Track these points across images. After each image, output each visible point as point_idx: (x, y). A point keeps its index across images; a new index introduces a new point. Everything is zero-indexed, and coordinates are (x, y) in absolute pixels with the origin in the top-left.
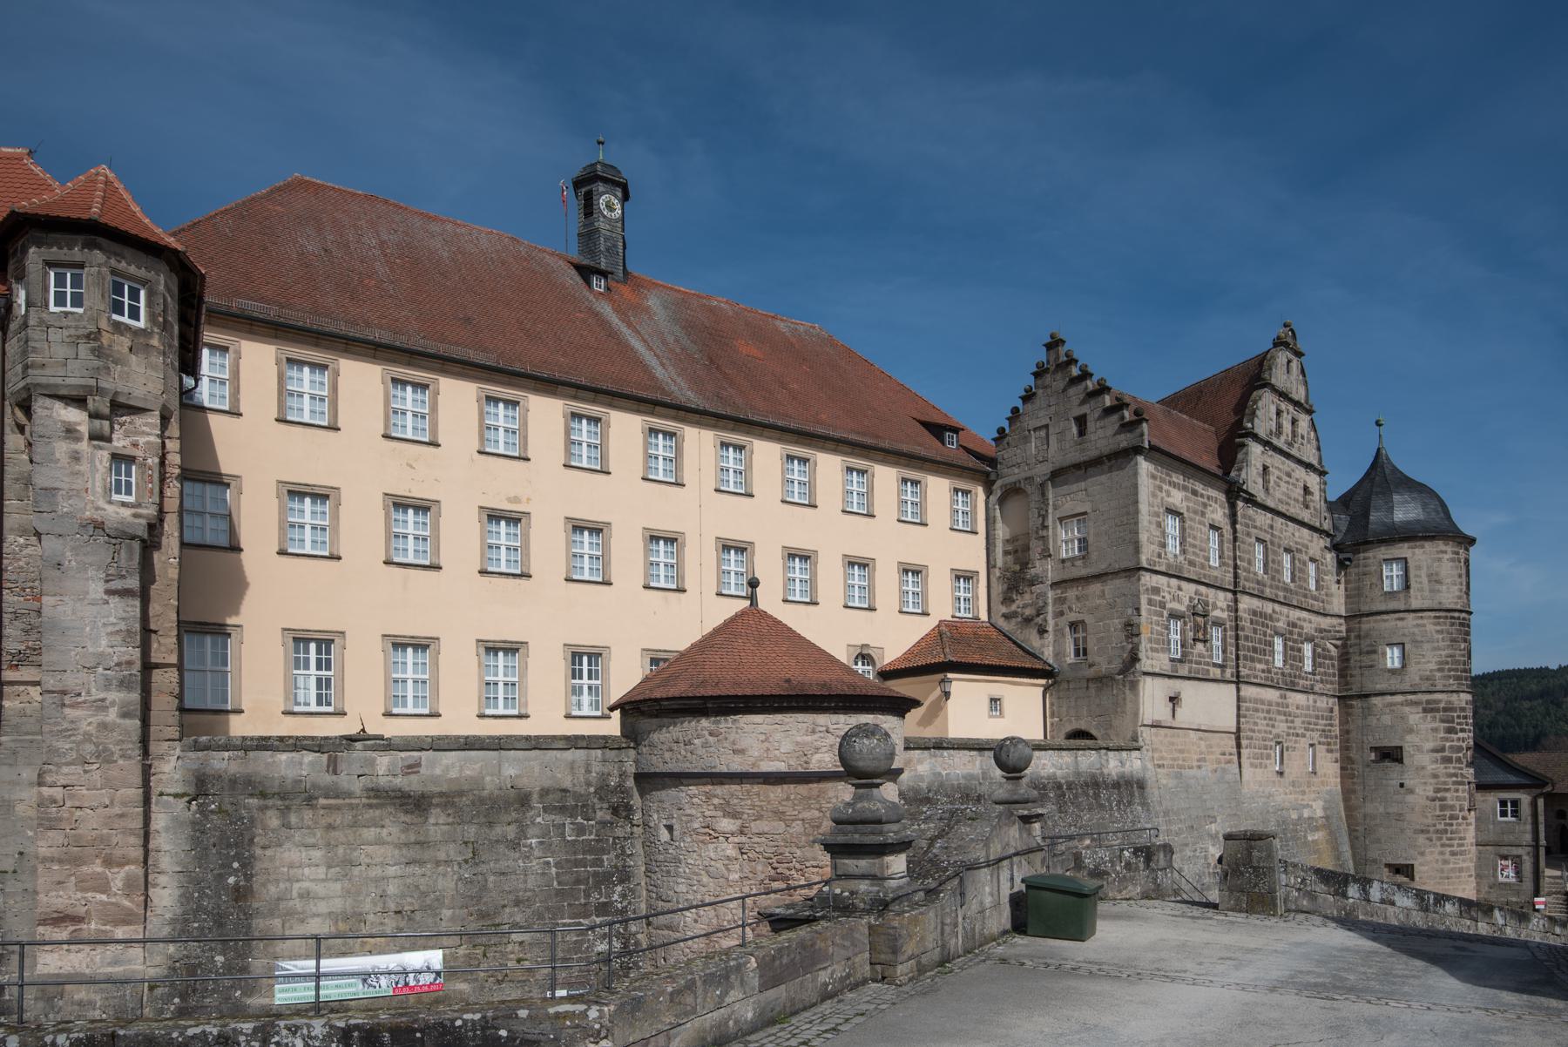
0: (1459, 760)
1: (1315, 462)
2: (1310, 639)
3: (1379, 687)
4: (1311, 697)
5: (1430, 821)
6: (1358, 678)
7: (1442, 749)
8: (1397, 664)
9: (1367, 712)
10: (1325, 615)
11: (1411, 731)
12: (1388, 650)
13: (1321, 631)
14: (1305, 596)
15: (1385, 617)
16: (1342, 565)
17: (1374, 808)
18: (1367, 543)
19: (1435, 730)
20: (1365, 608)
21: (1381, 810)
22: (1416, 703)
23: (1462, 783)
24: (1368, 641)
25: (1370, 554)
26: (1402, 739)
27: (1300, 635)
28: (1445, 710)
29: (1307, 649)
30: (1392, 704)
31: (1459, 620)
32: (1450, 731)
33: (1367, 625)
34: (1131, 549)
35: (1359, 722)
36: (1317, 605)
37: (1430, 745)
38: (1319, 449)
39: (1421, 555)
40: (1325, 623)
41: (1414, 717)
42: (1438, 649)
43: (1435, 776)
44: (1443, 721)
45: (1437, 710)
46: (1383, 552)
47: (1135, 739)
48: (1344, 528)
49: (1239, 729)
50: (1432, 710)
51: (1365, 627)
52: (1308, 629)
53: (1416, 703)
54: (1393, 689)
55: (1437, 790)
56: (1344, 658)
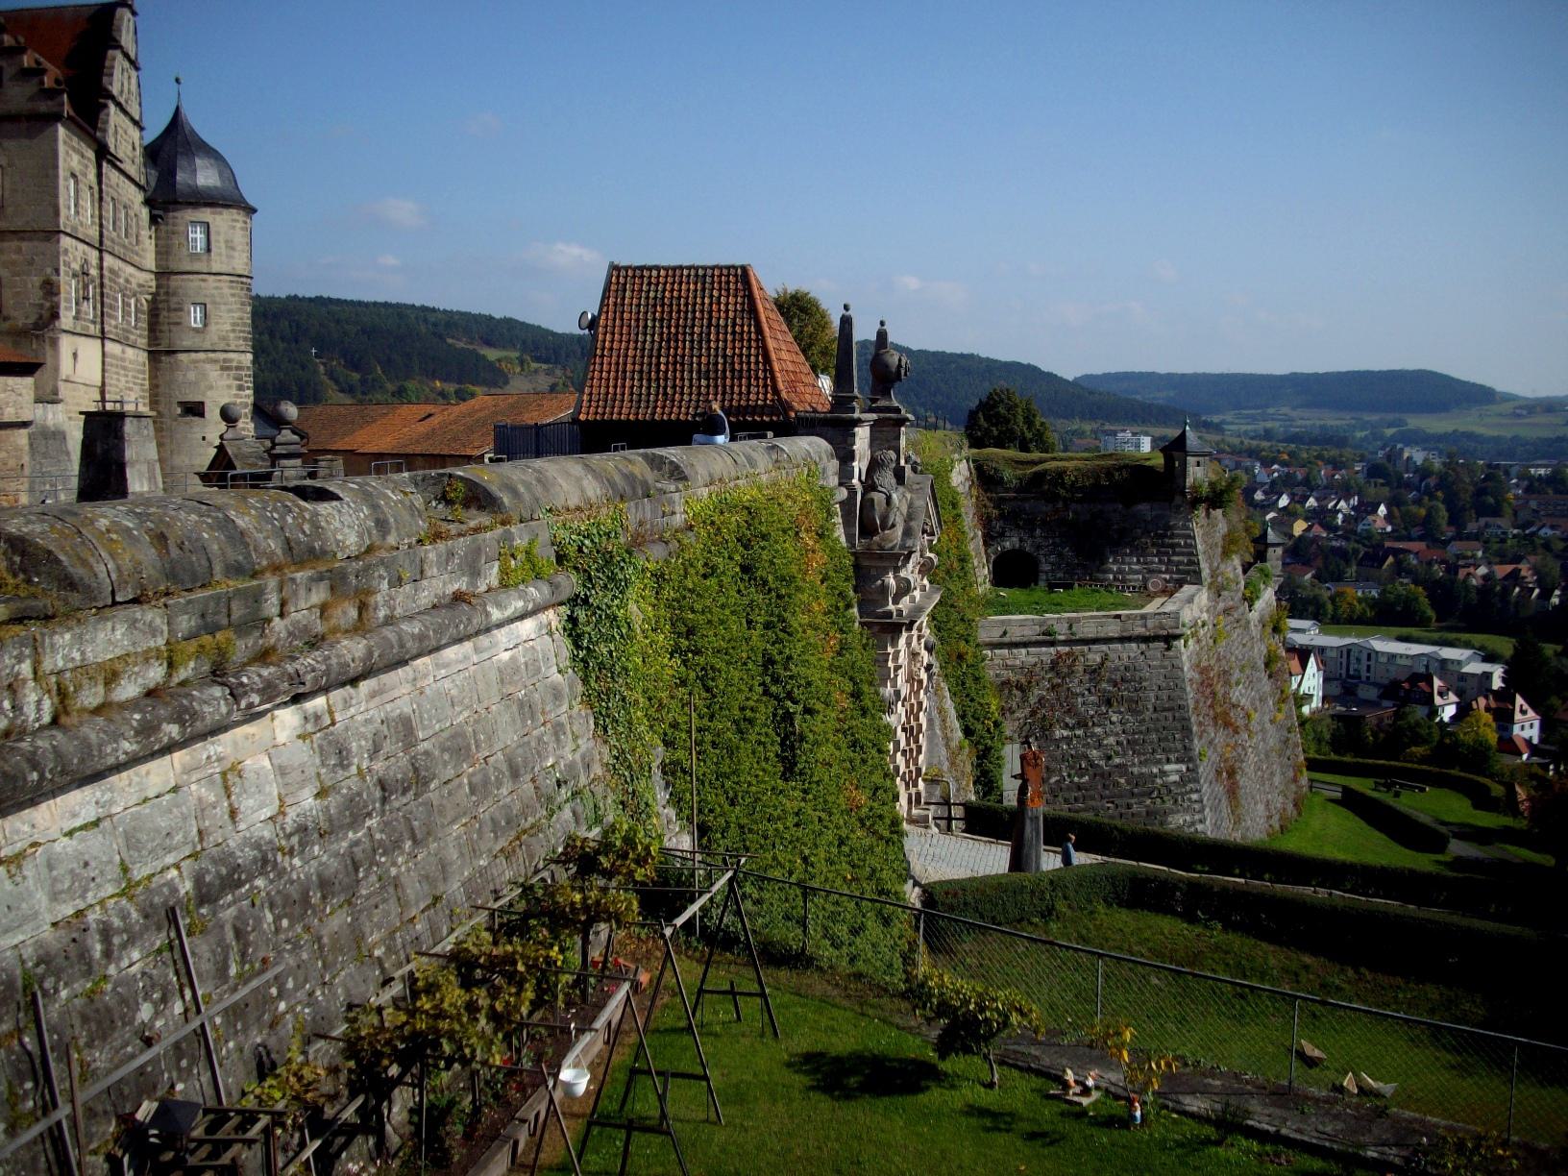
3: (186, 343)
11: (211, 388)
16: (154, 220)
18: (176, 202)
19: (229, 387)
25: (178, 214)
28: (238, 368)
30: (196, 362)
32: (240, 388)
33: (175, 282)
34: (51, 210)
39: (223, 221)
41: (214, 373)
42: (230, 311)
45: (228, 368)
46: (189, 215)
47: (56, 393)
49: (103, 384)
53: (216, 361)
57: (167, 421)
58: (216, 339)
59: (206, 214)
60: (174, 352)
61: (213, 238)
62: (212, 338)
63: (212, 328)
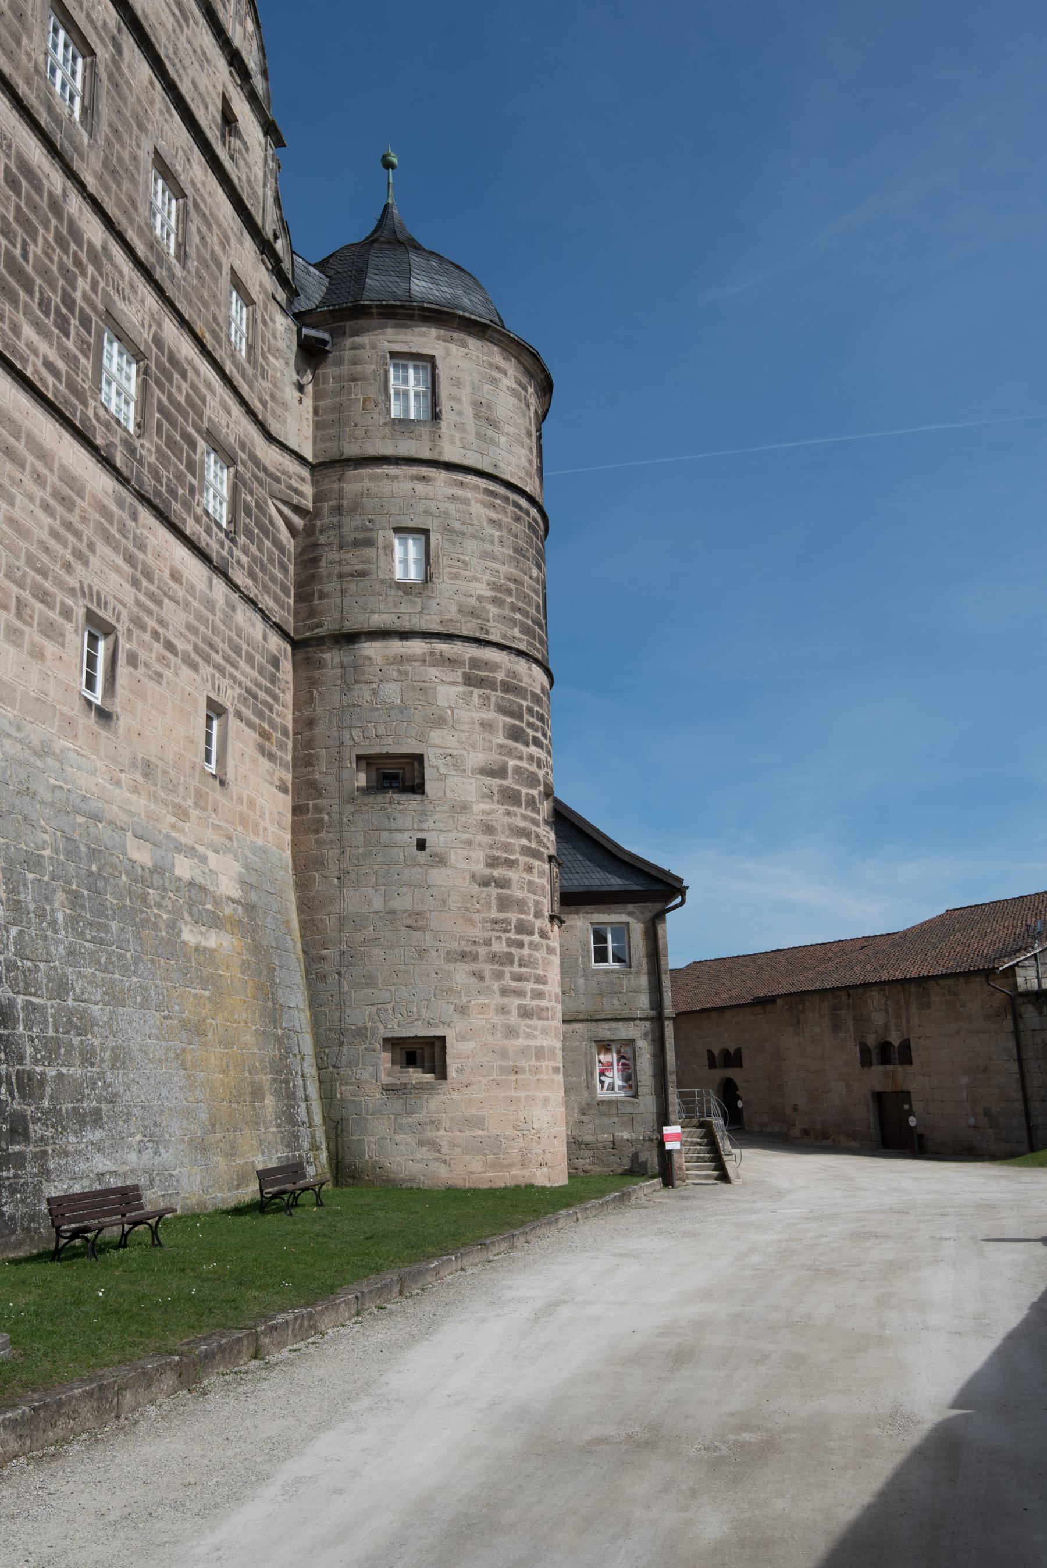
3: (379, 620)
5: (477, 932)
6: (334, 601)
7: (500, 772)
8: (414, 574)
9: (353, 675)
11: (440, 722)
13: (254, 458)
15: (392, 470)
16: (311, 354)
17: (362, 900)
19: (487, 726)
20: (352, 450)
21: (378, 904)
22: (452, 662)
23: (535, 854)
24: (357, 521)
25: (364, 339)
26: (422, 739)
28: (507, 687)
33: (357, 483)
37: (477, 758)
41: (448, 691)
43: (488, 829)
44: (502, 710)
53: (452, 662)
54: (406, 625)
55: (493, 862)
56: (308, 559)
57: (331, 803)
58: (452, 612)
59: (426, 339)
60: (350, 638)
61: (445, 390)
63: (444, 585)
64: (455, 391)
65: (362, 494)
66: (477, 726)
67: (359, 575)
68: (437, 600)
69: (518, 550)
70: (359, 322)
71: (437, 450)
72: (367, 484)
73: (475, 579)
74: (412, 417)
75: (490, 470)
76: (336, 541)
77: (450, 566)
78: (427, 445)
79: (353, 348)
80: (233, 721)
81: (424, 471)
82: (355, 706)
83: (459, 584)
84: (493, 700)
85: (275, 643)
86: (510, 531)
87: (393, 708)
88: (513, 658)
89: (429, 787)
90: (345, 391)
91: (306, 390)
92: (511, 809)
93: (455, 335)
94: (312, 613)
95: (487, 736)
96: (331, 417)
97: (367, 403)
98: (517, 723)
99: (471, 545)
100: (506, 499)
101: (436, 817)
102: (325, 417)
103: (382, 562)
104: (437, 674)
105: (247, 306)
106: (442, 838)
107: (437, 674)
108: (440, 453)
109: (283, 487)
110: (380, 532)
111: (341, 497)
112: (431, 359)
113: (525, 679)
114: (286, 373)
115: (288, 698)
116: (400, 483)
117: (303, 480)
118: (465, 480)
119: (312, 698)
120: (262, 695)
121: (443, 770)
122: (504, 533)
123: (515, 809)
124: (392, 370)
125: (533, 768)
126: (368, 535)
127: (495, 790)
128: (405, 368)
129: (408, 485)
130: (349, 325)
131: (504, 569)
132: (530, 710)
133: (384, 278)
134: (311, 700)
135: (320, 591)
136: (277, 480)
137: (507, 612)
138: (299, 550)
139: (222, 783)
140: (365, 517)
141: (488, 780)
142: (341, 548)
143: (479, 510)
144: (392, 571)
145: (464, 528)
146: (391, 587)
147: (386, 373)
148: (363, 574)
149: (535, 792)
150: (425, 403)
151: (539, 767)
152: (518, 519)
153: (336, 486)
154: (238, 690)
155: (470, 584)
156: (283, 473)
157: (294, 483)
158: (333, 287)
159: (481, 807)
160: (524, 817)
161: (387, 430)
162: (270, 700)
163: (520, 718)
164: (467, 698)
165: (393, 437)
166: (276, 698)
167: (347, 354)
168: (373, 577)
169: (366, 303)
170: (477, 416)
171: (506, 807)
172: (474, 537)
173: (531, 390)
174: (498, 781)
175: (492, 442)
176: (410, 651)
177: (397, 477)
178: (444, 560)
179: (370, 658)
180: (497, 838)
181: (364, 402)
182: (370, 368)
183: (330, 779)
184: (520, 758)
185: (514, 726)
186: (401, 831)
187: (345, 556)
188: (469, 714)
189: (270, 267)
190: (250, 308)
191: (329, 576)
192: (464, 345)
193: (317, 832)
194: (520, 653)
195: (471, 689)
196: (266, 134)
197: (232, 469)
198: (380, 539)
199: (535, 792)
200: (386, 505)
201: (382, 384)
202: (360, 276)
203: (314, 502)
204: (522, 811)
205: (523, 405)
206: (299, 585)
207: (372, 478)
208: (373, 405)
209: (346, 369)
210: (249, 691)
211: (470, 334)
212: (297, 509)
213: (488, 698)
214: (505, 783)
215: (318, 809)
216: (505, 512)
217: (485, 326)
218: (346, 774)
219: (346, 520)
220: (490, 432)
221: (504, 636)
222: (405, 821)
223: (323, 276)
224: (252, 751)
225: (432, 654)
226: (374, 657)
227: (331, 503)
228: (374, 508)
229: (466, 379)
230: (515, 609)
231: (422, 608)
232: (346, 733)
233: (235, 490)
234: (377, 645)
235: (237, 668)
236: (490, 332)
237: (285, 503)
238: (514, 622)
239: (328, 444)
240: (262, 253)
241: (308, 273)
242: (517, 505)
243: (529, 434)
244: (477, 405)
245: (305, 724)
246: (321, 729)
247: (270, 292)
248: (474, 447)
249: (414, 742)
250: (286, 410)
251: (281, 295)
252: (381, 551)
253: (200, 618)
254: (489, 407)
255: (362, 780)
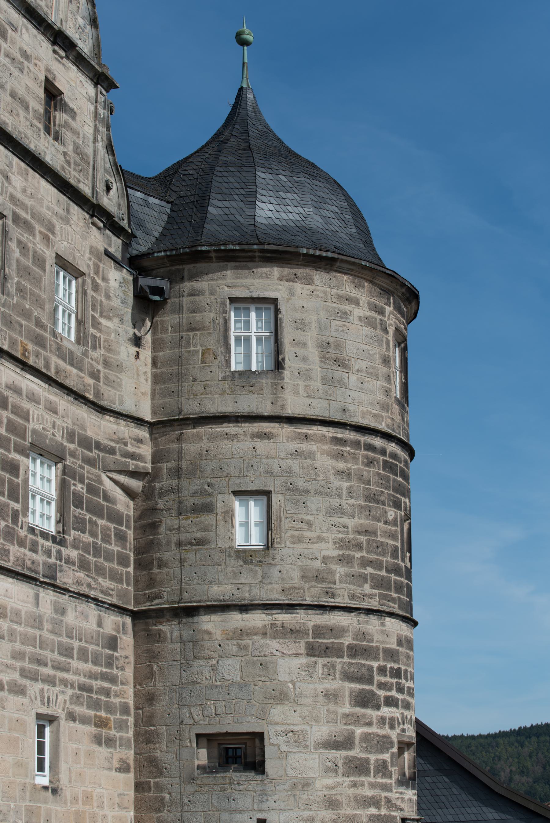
0: (382, 769)
1: (85, 47)
2: (52, 455)
3: (219, 591)
4: (48, 597)
6: (173, 570)
7: (347, 743)
10: (103, 410)
11: (281, 697)
12: (237, 505)
13: (86, 443)
14: (40, 341)
15: (231, 428)
16: (147, 304)
18: (198, 257)
19: (332, 697)
20: (191, 408)
22: (294, 633)
24: (195, 484)
25: (203, 284)
26: (262, 716)
27: (12, 427)
28: (355, 651)
29: (42, 479)
31: (388, 452)
32: (365, 700)
33: (197, 443)
35: (175, 674)
36: (74, 377)
37: (321, 731)
38: (94, 22)
39: (314, 301)
40: (101, 428)
41: (290, 664)
43: (332, 803)
44: (349, 677)
45: (336, 651)
48: (157, 229)
50: (327, 651)
51: (190, 449)
52: (39, 421)
53: (294, 633)
54: (245, 596)
56: (148, 522)
57: (171, 781)
59: (268, 281)
61: (288, 335)
62: (286, 575)
63: (286, 550)
64: (299, 335)
65: (201, 456)
66: (321, 698)
67: (198, 544)
68: (279, 568)
69: (371, 497)
70: (198, 265)
71: (279, 404)
72: (206, 445)
73: (320, 539)
74: (254, 369)
75: (337, 417)
76: (175, 507)
77: (293, 528)
78: (268, 397)
79: (191, 295)
80: (64, 725)
81: (265, 427)
82: (194, 683)
83: (302, 548)
84: (339, 667)
85: (112, 621)
86: (360, 478)
87: (232, 685)
88: (363, 618)
89: (269, 766)
90: (184, 342)
91: (143, 341)
92: (358, 779)
93: (300, 272)
94: (152, 583)
95: (332, 707)
96: (168, 370)
97: (207, 355)
98: (367, 687)
99: (316, 503)
100: (357, 444)
101: (276, 797)
102: (163, 370)
103: (221, 530)
104: (278, 647)
105: (76, 278)
106: (282, 817)
107: (278, 647)
108: (283, 407)
109: (118, 457)
110: (220, 497)
111: (180, 459)
112: (274, 301)
113: (377, 637)
114: (120, 331)
115: (129, 673)
116: (239, 443)
117: (140, 441)
118: (310, 432)
119: (152, 672)
120: (97, 684)
121: (284, 748)
122: (354, 483)
123: (363, 778)
124: (232, 314)
125: (386, 731)
126: (207, 500)
127: (340, 762)
128: (248, 310)
129: (249, 444)
130: (187, 267)
131: (351, 523)
132: (382, 670)
133: (227, 204)
134: (151, 675)
135: (159, 559)
136: (111, 451)
137: (356, 569)
138: (138, 513)
139: (55, 791)
140: (204, 481)
141: (333, 754)
142: (180, 514)
143: (325, 462)
144: (231, 539)
145: (308, 486)
146: (230, 556)
147: (226, 322)
148: (201, 542)
149: (386, 756)
150: (267, 348)
151: (392, 727)
152: (370, 463)
153: (174, 446)
154: (70, 692)
155: (315, 546)
156: (117, 442)
157: (130, 448)
158: (174, 215)
159: (324, 783)
160: (373, 786)
161: (226, 385)
162: (106, 685)
163: (370, 681)
164: (310, 669)
165: (232, 392)
166: (113, 680)
167: (186, 301)
168: (212, 545)
169: (204, 248)
170: (323, 359)
171: (352, 779)
172: (319, 493)
173: (389, 309)
174: (344, 753)
175: (342, 384)
176: (250, 625)
177: (236, 436)
178: (286, 524)
179: (208, 633)
180: (342, 812)
181: (203, 355)
182: (209, 316)
183: (170, 758)
184: (370, 724)
185: (362, 691)
186: (241, 812)
187: (184, 523)
188: (312, 686)
189: (101, 225)
190: (80, 280)
191: (168, 543)
192: (309, 281)
193: (159, 810)
194: (370, 612)
195: (313, 659)
196: (96, 85)
197: (60, 466)
198: (220, 504)
199: (386, 756)
200: (225, 467)
201: (222, 334)
202: (202, 203)
203: (153, 463)
204: (371, 779)
205: (379, 332)
206: (140, 551)
207: (212, 438)
208: (212, 357)
209: (185, 318)
210: (83, 688)
211: (316, 268)
212: (134, 474)
213: (333, 667)
214: (351, 753)
215: (159, 788)
216: (355, 458)
217: (332, 260)
218: (186, 753)
219: (184, 483)
220: (339, 374)
221: (353, 597)
222: (245, 802)
223: (164, 204)
224: (86, 745)
225: (273, 625)
226: (213, 631)
227: (170, 464)
228: (213, 470)
229: (312, 319)
230: (365, 563)
231: (263, 577)
232: (185, 711)
233: (63, 486)
234: (216, 618)
235: (67, 670)
236: (338, 264)
237: (120, 472)
238: (364, 578)
239: (167, 400)
240: (92, 216)
241: (147, 204)
242: (370, 447)
243: (386, 361)
244: (324, 346)
245: (146, 699)
246: (161, 706)
247: (102, 250)
248: (320, 394)
249: (254, 720)
250: (121, 372)
251: (116, 245)
252: (220, 517)
253: (27, 640)
254: (338, 346)
255: (202, 757)
